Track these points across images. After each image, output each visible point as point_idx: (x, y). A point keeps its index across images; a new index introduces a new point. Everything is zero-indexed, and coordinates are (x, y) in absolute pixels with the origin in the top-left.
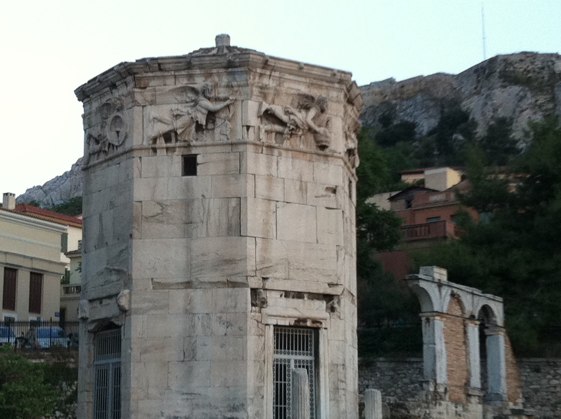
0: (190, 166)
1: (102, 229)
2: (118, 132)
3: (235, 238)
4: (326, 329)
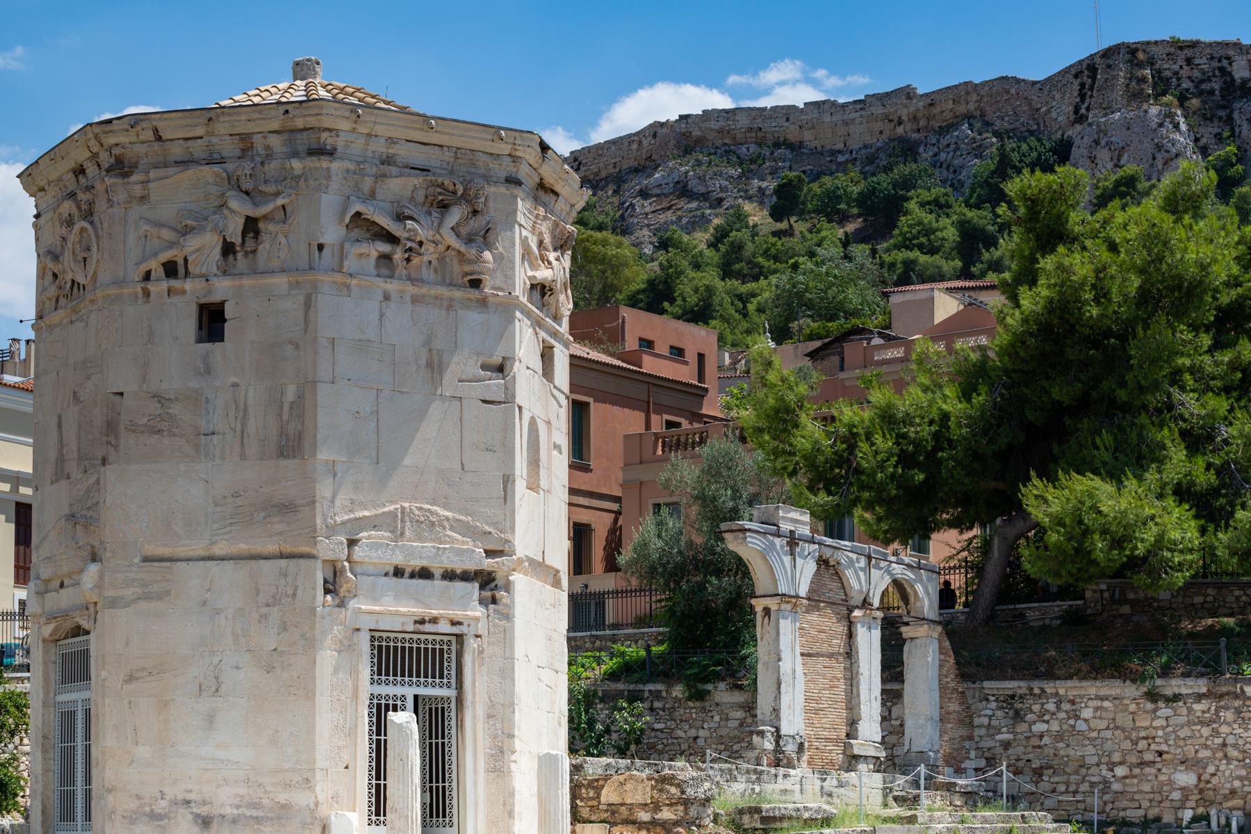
0: (212, 321)
1: (61, 444)
2: (85, 259)
3: (290, 463)
4: (477, 636)
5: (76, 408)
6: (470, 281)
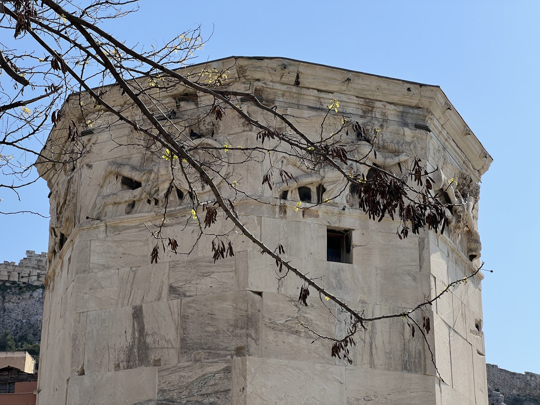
3: (415, 377)
5: (175, 302)
6: (470, 256)
